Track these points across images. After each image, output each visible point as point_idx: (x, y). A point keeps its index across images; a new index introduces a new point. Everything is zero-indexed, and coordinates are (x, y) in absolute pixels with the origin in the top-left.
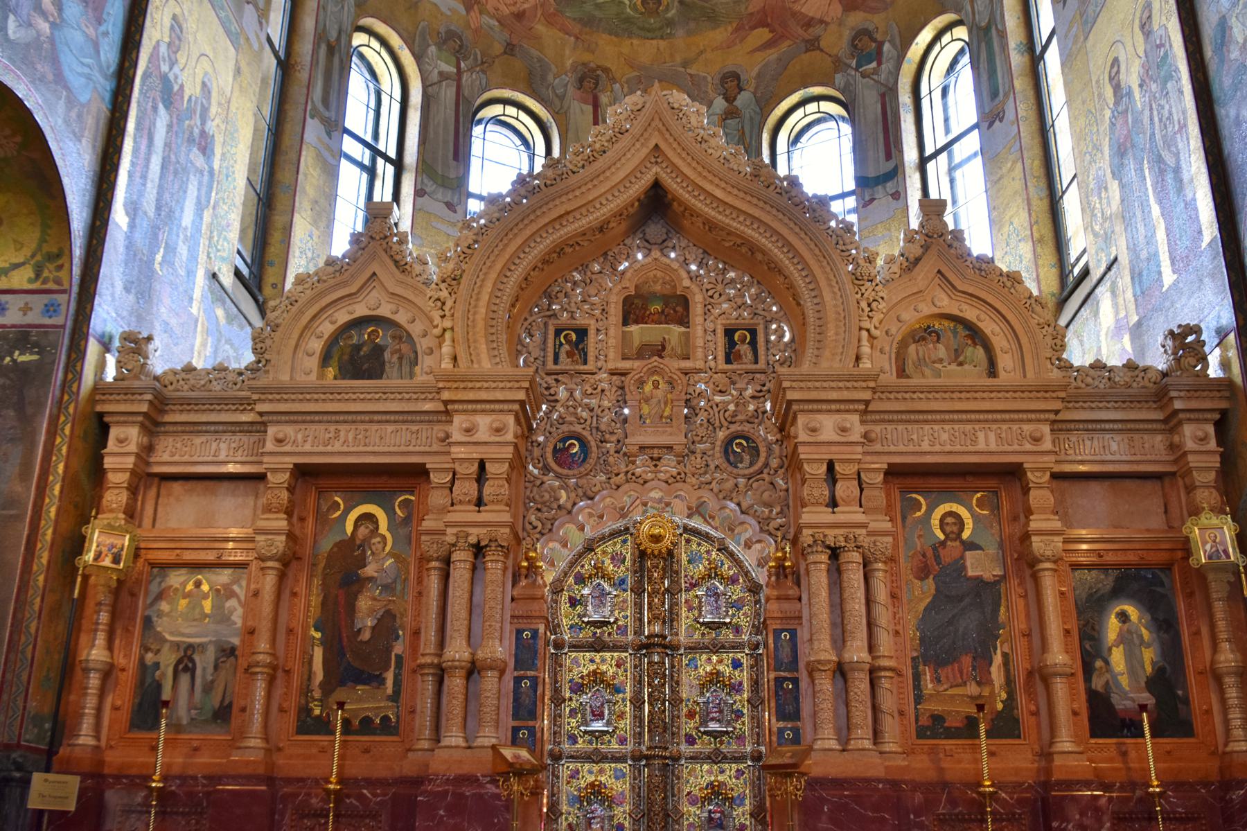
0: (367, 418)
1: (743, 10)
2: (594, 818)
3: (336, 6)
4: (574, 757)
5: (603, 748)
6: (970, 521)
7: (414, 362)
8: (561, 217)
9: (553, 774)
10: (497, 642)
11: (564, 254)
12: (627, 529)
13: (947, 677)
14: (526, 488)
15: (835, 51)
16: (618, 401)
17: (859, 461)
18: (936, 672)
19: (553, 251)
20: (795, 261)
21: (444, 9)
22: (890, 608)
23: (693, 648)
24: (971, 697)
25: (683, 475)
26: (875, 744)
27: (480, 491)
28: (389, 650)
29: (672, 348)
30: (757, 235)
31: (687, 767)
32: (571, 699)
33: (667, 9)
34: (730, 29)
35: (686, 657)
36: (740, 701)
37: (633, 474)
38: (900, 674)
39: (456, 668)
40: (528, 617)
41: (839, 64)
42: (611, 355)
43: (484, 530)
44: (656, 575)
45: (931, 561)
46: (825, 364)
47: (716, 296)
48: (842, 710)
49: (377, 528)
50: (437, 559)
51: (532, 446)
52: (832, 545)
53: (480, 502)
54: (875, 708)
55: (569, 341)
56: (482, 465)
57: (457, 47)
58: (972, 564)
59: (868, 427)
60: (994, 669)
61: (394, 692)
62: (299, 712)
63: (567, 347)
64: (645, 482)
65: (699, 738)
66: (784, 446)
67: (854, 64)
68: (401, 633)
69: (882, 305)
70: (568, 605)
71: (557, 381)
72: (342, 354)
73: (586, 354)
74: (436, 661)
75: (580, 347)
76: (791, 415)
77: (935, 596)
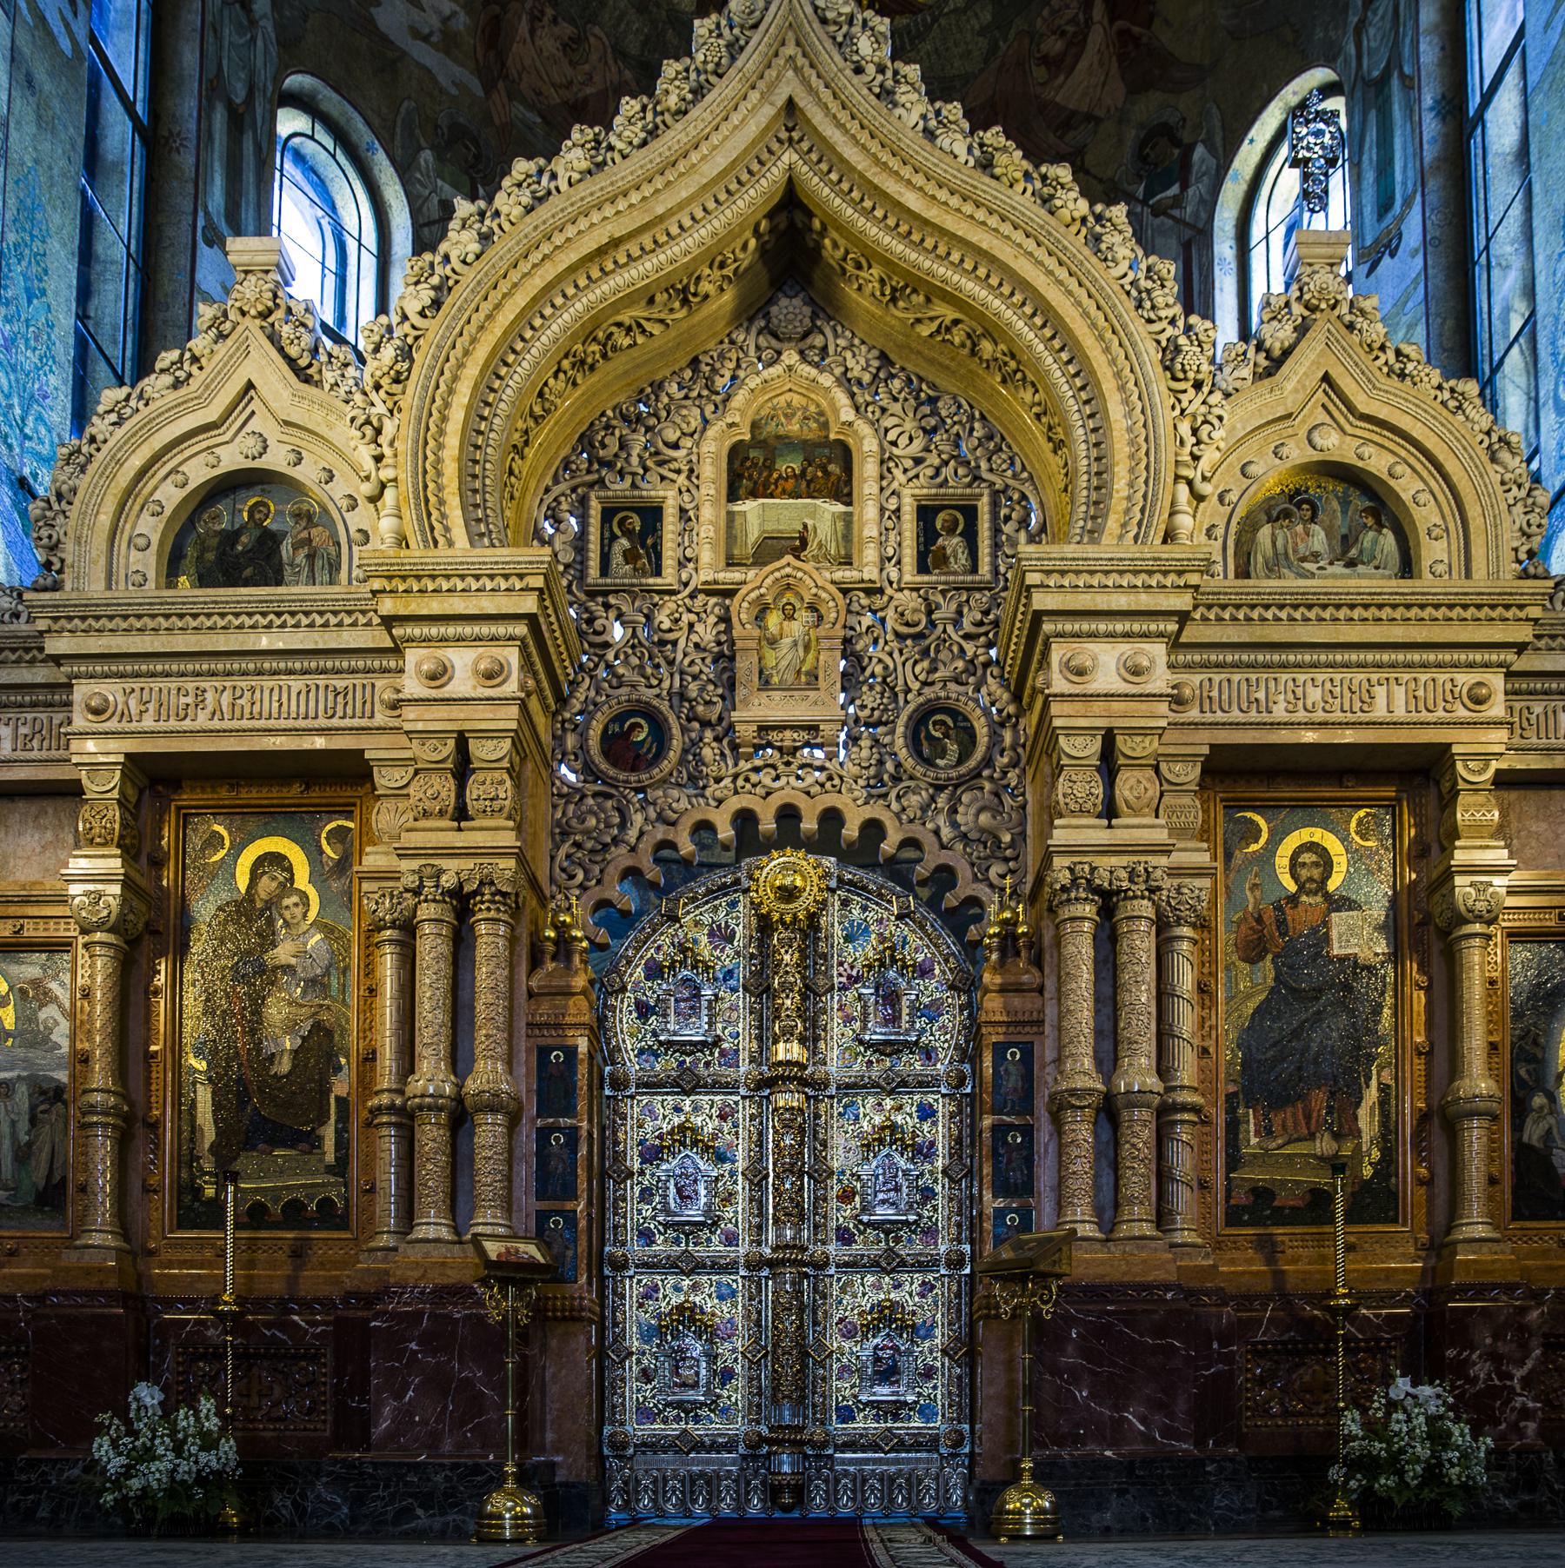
2: (683, 1359)
4: (648, 1266)
6: (1343, 860)
7: (334, 567)
9: (615, 1293)
11: (615, 349)
13: (1284, 1126)
18: (1266, 1116)
19: (590, 337)
23: (850, 1088)
24: (1321, 1158)
28: (325, 1091)
44: (787, 958)
45: (1271, 928)
48: (1107, 1179)
58: (1340, 936)
60: (1363, 1113)
62: (180, 1193)
65: (861, 1233)
68: (343, 1061)
72: (203, 550)
77: (1273, 991)
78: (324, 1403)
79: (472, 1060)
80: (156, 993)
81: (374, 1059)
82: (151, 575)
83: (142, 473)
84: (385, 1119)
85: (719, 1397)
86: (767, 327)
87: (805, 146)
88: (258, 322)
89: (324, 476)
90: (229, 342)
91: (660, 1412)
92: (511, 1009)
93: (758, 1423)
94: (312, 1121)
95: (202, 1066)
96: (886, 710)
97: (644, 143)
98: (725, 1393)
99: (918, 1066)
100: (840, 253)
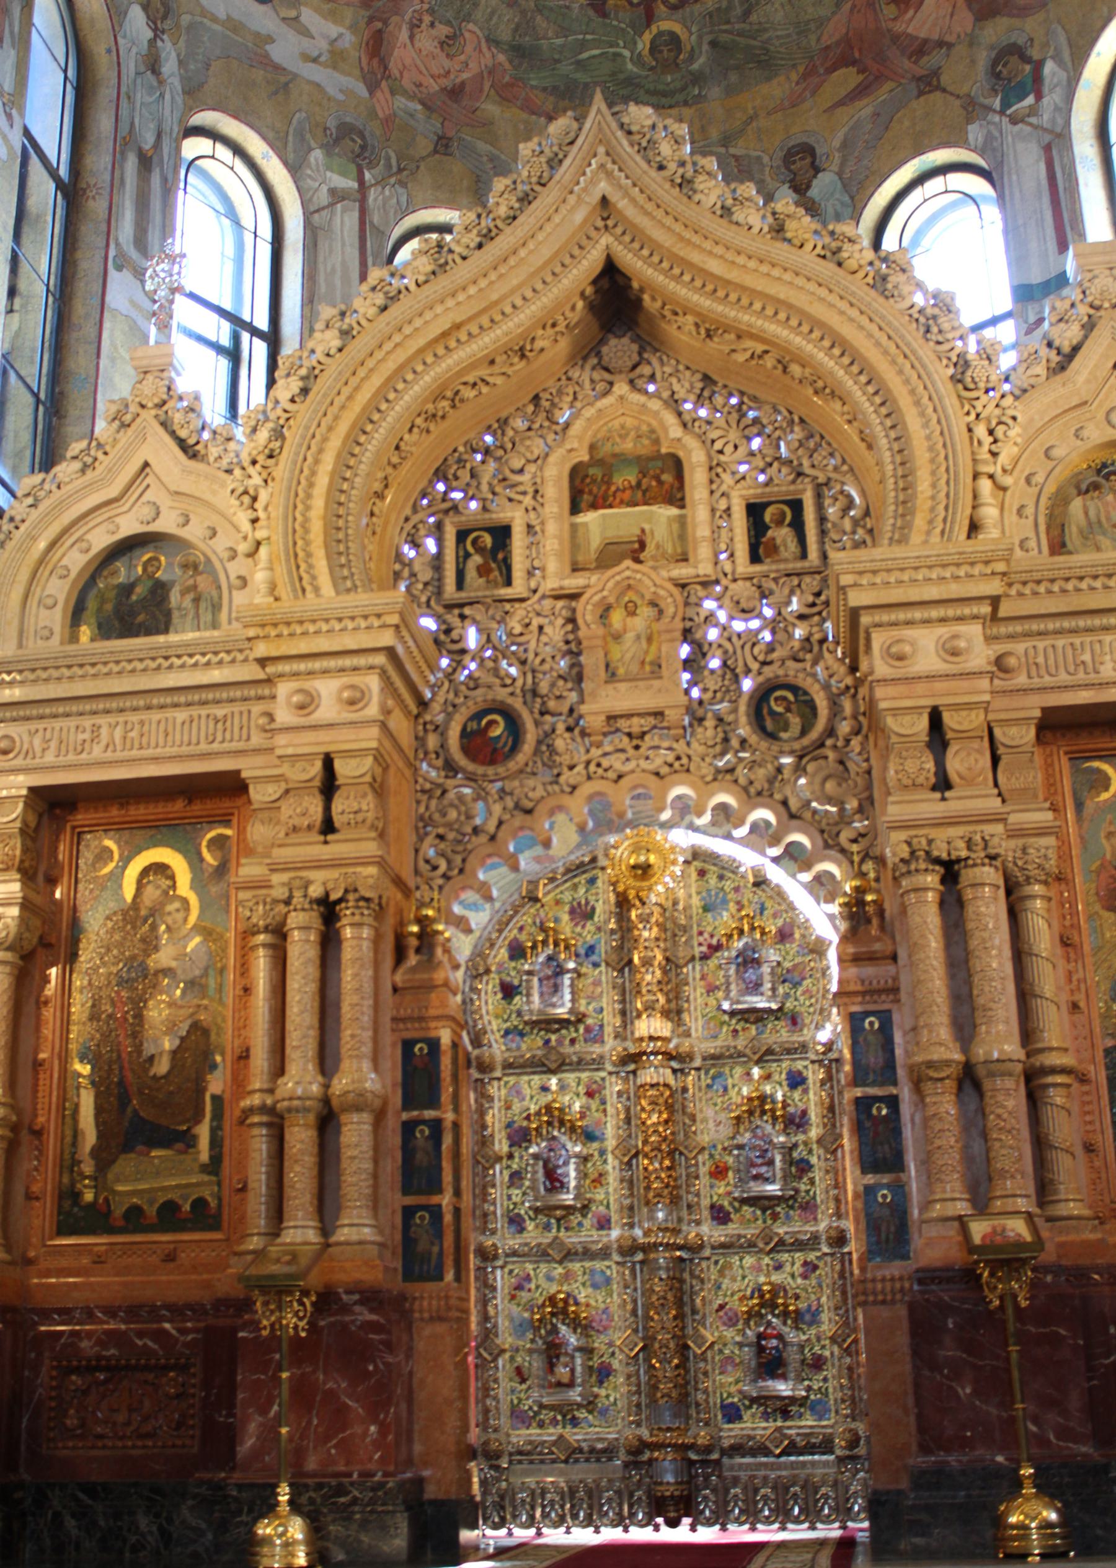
0: (142, 703)
1: (813, 43)
3: (150, 95)
5: (571, 1239)
7: (216, 607)
8: (445, 335)
10: (366, 1065)
11: (462, 401)
12: (594, 860)
14: (418, 802)
15: (965, 89)
16: (567, 642)
17: (986, 707)
19: (439, 396)
20: (855, 369)
21: (331, 91)
22: (1061, 963)
25: (685, 761)
26: (1041, 1204)
27: (327, 809)
28: (201, 1091)
29: (658, 547)
30: (785, 333)
31: (716, 1262)
32: (510, 1156)
33: (691, 58)
34: (794, 76)
35: (706, 1073)
36: (805, 1143)
37: (599, 765)
38: (1083, 1079)
39: (297, 1111)
40: (421, 1019)
41: (972, 109)
42: (552, 566)
43: (334, 874)
46: (916, 538)
47: (729, 449)
49: (174, 887)
50: (266, 930)
51: (426, 730)
52: (944, 856)
53: (328, 827)
54: (1040, 1143)
55: (480, 550)
56: (328, 762)
57: (357, 149)
59: (1000, 648)
61: (211, 1157)
63: (477, 559)
64: (620, 777)
66: (860, 696)
67: (997, 104)
68: (218, 1058)
69: (1015, 432)
70: (500, 996)
71: (463, 617)
72: (103, 601)
73: (509, 569)
74: (269, 1102)
75: (500, 556)
76: (862, 635)
78: (193, 1416)
79: (337, 1060)
80: (46, 1003)
81: (247, 1057)
82: (57, 629)
83: (52, 545)
84: (256, 1119)
85: (596, 1396)
86: (599, 363)
87: (619, 230)
88: (153, 412)
89: (208, 533)
90: (130, 431)
91: (536, 1414)
92: (376, 1007)
93: (638, 1424)
94: (188, 1121)
95: (85, 1069)
96: (728, 691)
97: (480, 246)
98: (603, 1392)
99: (784, 1032)
100: (659, 304)
